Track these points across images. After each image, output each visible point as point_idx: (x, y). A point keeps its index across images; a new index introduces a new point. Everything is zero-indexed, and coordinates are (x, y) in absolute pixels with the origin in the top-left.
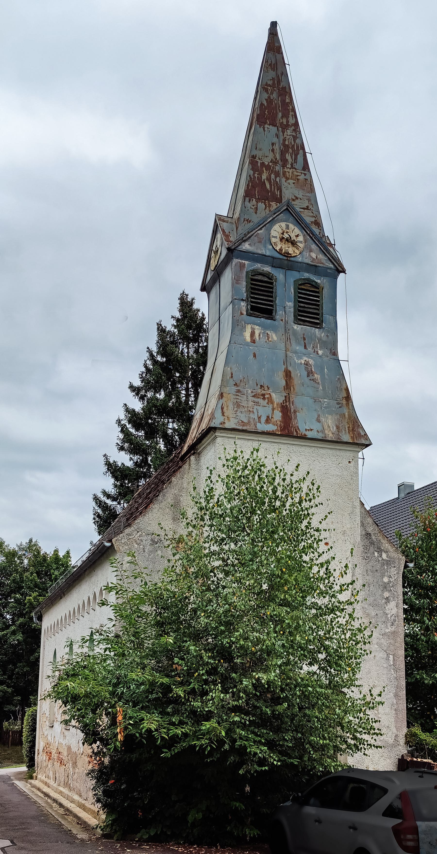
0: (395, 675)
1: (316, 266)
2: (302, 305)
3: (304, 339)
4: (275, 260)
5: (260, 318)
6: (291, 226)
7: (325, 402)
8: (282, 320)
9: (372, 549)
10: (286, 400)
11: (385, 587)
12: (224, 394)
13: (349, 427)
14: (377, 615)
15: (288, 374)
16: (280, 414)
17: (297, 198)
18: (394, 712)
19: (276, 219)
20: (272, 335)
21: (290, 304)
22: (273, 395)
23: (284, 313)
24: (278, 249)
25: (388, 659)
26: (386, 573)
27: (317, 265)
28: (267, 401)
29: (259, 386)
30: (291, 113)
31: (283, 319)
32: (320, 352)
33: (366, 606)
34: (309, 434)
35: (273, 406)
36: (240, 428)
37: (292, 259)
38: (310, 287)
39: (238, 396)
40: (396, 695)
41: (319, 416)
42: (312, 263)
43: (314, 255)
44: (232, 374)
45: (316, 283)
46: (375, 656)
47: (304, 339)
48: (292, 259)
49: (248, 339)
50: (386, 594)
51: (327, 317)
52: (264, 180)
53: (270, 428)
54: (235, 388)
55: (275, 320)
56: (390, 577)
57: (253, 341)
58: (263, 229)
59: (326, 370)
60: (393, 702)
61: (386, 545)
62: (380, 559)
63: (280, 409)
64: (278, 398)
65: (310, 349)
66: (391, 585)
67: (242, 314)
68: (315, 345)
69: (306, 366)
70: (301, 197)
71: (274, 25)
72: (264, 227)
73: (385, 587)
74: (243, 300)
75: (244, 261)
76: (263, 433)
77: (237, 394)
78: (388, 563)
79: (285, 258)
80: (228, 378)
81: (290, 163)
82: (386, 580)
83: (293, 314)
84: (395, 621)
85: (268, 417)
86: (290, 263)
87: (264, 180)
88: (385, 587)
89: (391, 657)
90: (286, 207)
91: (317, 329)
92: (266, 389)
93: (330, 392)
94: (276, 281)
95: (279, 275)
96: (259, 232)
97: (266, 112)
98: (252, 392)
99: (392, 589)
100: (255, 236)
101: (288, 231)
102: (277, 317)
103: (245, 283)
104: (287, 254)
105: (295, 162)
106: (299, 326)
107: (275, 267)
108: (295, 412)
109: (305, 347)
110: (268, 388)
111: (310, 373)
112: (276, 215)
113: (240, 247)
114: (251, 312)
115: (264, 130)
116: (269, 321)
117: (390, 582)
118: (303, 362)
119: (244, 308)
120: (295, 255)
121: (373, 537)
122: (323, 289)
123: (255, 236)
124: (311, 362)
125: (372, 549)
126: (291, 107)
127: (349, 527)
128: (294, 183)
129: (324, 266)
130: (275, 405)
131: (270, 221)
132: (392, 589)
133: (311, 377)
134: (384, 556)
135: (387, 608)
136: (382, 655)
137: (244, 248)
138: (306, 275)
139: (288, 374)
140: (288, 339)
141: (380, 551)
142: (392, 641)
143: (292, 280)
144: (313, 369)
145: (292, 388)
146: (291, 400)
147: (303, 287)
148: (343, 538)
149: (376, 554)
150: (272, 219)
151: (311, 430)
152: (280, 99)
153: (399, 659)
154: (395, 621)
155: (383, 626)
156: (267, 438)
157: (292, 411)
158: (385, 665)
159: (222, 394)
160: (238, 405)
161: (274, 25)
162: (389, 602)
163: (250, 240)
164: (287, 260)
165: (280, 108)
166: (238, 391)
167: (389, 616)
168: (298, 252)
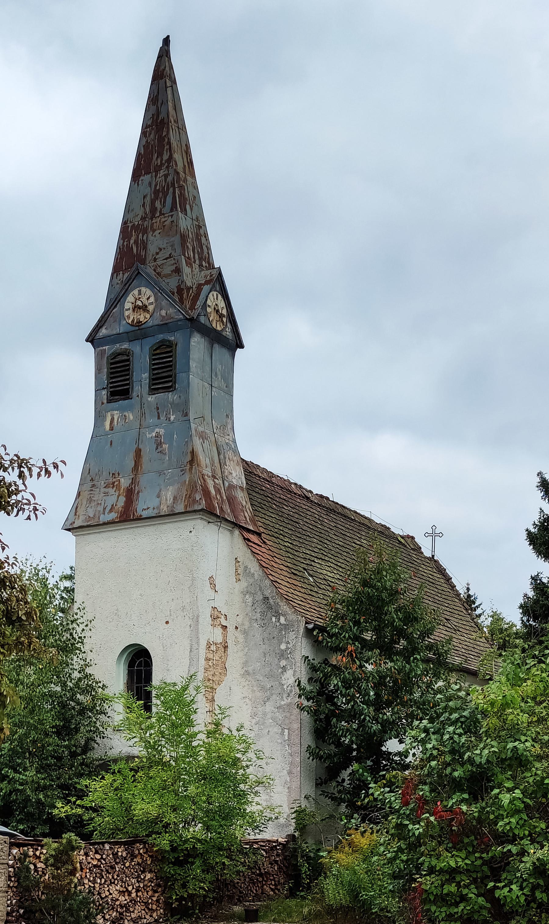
0: (290, 751)
1: (166, 324)
2: (156, 372)
3: (158, 408)
6: (143, 289)
7: (169, 473)
8: (138, 396)
9: (269, 614)
11: (282, 655)
13: (186, 495)
14: (272, 686)
15: (138, 453)
16: (125, 499)
17: (160, 249)
18: (287, 790)
20: (129, 416)
21: (146, 375)
22: (122, 480)
25: (282, 734)
26: (284, 639)
27: (167, 322)
29: (111, 475)
30: (166, 147)
32: (172, 418)
33: (261, 678)
34: (145, 514)
36: (85, 524)
37: (143, 326)
38: (165, 348)
40: (290, 773)
41: (160, 491)
42: (162, 323)
43: (163, 313)
44: (89, 470)
45: (169, 341)
46: (269, 731)
47: (158, 408)
48: (143, 326)
49: (107, 427)
50: (283, 663)
51: (181, 376)
53: (113, 516)
55: (131, 399)
56: (288, 643)
57: (112, 429)
58: (118, 305)
59: (175, 436)
60: (286, 781)
61: (284, 607)
62: (278, 624)
64: (125, 482)
66: (289, 652)
67: (103, 403)
69: (156, 438)
70: (164, 246)
73: (282, 655)
75: (104, 348)
76: (104, 524)
78: (286, 627)
79: (137, 328)
81: (159, 210)
82: (283, 647)
84: (291, 691)
85: (113, 505)
86: (143, 331)
88: (282, 655)
89: (286, 731)
91: (171, 393)
92: (117, 475)
93: (175, 460)
94: (133, 356)
95: (136, 348)
96: (114, 311)
97: (142, 162)
98: (105, 483)
99: (289, 656)
101: (140, 296)
103: (106, 370)
107: (131, 341)
108: (138, 493)
109: (159, 418)
110: (119, 474)
111: (159, 444)
112: (128, 284)
113: (97, 335)
115: (138, 185)
116: (126, 401)
117: (288, 648)
119: (105, 397)
120: (146, 320)
121: (271, 601)
122: (176, 345)
124: (162, 431)
125: (269, 614)
126: (166, 140)
127: (188, 601)
128: (159, 233)
130: (122, 491)
132: (289, 656)
133: (159, 450)
134: (282, 620)
135: (283, 678)
136: (277, 729)
137: (101, 334)
138: (161, 337)
139: (138, 453)
140: (143, 414)
141: (278, 615)
142: (288, 714)
143: (147, 349)
144: (162, 440)
145: (140, 468)
147: (158, 351)
148: (182, 613)
149: (274, 619)
150: (126, 291)
153: (294, 733)
154: (291, 691)
155: (278, 698)
157: (136, 492)
158: (279, 741)
160: (90, 500)
162: (285, 671)
163: (106, 324)
164: (139, 329)
165: (156, 148)
166: (93, 486)
167: (285, 687)
168: (148, 316)
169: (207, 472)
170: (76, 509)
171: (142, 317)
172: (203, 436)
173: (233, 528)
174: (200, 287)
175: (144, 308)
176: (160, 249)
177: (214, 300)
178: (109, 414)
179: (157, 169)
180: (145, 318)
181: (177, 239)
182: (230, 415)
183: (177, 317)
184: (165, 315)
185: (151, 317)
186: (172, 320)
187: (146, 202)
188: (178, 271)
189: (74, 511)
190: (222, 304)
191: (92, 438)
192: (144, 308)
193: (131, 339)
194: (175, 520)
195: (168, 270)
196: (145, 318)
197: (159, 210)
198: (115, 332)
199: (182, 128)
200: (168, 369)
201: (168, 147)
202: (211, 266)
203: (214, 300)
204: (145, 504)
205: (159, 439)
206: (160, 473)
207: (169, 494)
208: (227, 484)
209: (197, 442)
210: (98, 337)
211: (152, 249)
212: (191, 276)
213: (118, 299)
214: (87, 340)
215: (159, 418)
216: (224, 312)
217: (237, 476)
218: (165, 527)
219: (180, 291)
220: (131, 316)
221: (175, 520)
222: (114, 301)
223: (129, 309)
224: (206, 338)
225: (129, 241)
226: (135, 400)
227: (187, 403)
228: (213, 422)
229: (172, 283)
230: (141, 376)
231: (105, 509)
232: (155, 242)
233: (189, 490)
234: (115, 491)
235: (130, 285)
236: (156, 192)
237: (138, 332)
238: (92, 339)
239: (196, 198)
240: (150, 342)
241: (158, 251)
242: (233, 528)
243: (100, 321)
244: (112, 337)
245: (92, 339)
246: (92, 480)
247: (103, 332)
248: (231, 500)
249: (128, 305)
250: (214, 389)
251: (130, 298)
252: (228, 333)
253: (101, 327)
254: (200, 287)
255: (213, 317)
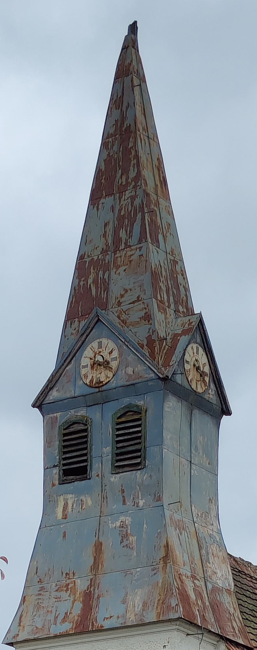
2: (121, 445)
3: (123, 491)
4: (87, 397)
5: (74, 482)
6: (104, 341)
7: (137, 572)
8: (98, 476)
10: (91, 584)
12: (26, 598)
13: (159, 600)
15: (98, 547)
16: (81, 605)
17: (126, 291)
19: (87, 340)
20: (86, 500)
21: (108, 450)
22: (78, 582)
23: (100, 465)
24: (88, 382)
27: (134, 382)
28: (69, 592)
29: (64, 575)
30: (132, 162)
31: (100, 473)
32: (141, 503)
34: (107, 624)
35: (74, 598)
36: (32, 637)
37: (104, 388)
39: (41, 594)
41: (126, 595)
42: (128, 383)
43: (130, 370)
44: (37, 570)
45: (137, 406)
47: (123, 491)
51: (151, 451)
52: (90, 286)
53: (67, 627)
54: (39, 586)
55: (90, 479)
57: (65, 517)
58: (73, 361)
59: (145, 525)
63: (81, 599)
64: (82, 585)
65: (129, 503)
67: (53, 485)
68: (136, 494)
69: (121, 529)
70: (131, 287)
71: (133, 28)
72: (74, 358)
74: (55, 466)
76: (56, 637)
77: (40, 592)
79: (97, 390)
80: (33, 575)
81: (124, 241)
83: (110, 462)
85: (66, 613)
86: (104, 393)
87: (90, 286)
90: (97, 319)
91: (139, 472)
93: (145, 556)
94: (91, 426)
96: (67, 368)
97: (103, 181)
100: (64, 376)
101: (100, 350)
102: (94, 473)
103: (57, 443)
104: (99, 384)
105: (129, 238)
106: (117, 475)
107: (90, 406)
108: (99, 597)
109: (124, 503)
111: (125, 537)
112: (85, 335)
113: (47, 399)
114: (65, 478)
116: (83, 482)
118: (118, 524)
119: (57, 476)
120: (108, 380)
122: (146, 411)
123: (64, 376)
124: (128, 520)
126: (133, 153)
128: (125, 270)
129: (144, 380)
130: (78, 595)
131: (80, 346)
133: (125, 543)
137: (51, 398)
138: (126, 401)
139: (98, 547)
140: (104, 498)
143: (110, 415)
144: (129, 531)
145: (100, 566)
146: (97, 582)
147: (123, 419)
150: (83, 343)
151: (111, 617)
152: (121, 149)
156: (90, 637)
159: (25, 597)
160: (38, 607)
161: (133, 28)
163: (58, 385)
164: (99, 391)
165: (121, 163)
166: (42, 589)
168: (110, 375)
169: (186, 571)
170: (20, 618)
171: (103, 376)
172: (180, 527)
173: (218, 642)
174: (176, 338)
175: (106, 365)
176: (126, 291)
177: (194, 354)
178: (62, 498)
179: (122, 190)
180: (107, 377)
181: (146, 278)
182: (214, 499)
183: (147, 376)
184: (132, 373)
185: (114, 375)
186: (140, 380)
187: (108, 231)
188: (148, 318)
189: (18, 620)
190: (203, 359)
191: (40, 528)
192: (106, 365)
193: (88, 404)
194: (145, 632)
195: (135, 315)
196: (107, 377)
197: (124, 241)
198: (68, 396)
199: (152, 138)
200: (136, 441)
201: (135, 161)
202: (189, 311)
203: (194, 354)
204: (106, 612)
205: (125, 530)
206: (126, 572)
207: (137, 600)
208: (210, 586)
209: (173, 534)
210: (47, 401)
211: (115, 290)
212: (165, 324)
213: (72, 354)
214: (34, 406)
215: (124, 503)
216: (207, 369)
217: (223, 577)
218: (132, 640)
219: (150, 343)
220: (90, 375)
221: (145, 632)
222: (68, 357)
223: (86, 366)
224: (184, 403)
225: (86, 280)
226: (94, 481)
227: (159, 483)
228: (193, 508)
229: (141, 333)
230: (102, 449)
231: (56, 618)
232: (120, 281)
233: (162, 594)
234: (69, 596)
235: (87, 336)
236: (121, 219)
237: (99, 395)
238: (39, 404)
239: (171, 226)
240: (113, 409)
241: (123, 293)
242: (218, 642)
243: (50, 381)
244: (66, 401)
245: (39, 404)
246: (40, 581)
247: (54, 395)
248: (216, 607)
249: (85, 361)
250: (193, 467)
251: (88, 353)
252: (212, 396)
253: (51, 389)
254: (176, 338)
255: (193, 375)
